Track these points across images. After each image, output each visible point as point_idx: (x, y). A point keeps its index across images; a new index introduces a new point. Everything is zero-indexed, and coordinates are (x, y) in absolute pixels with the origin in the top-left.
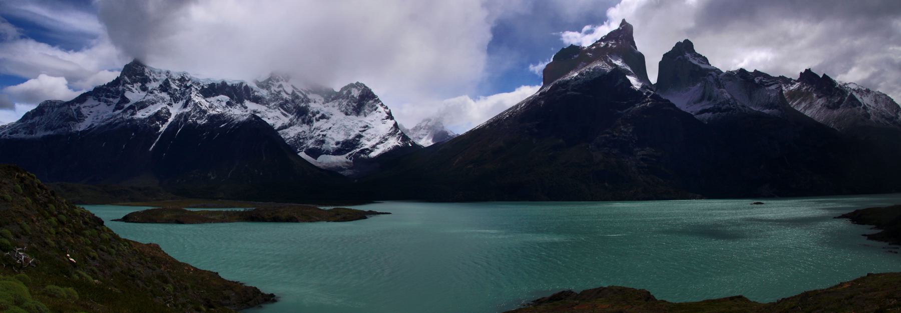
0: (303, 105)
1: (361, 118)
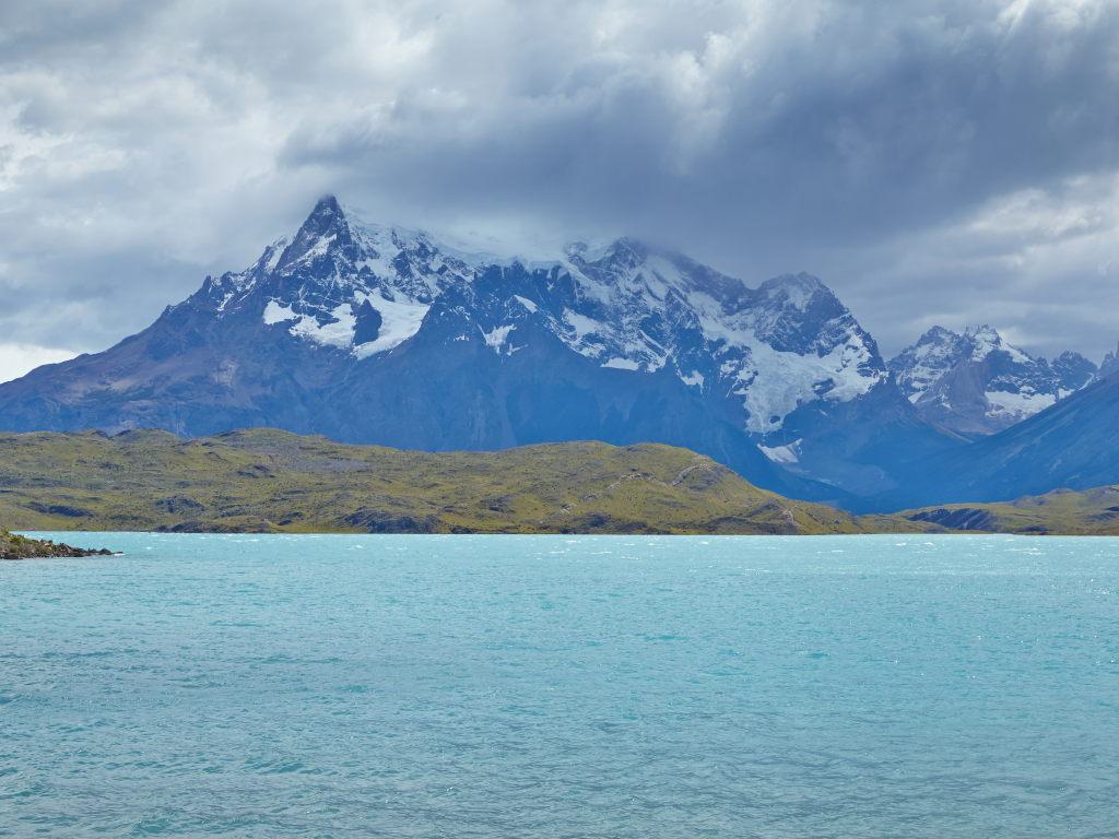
0: (688, 325)
1: (812, 359)
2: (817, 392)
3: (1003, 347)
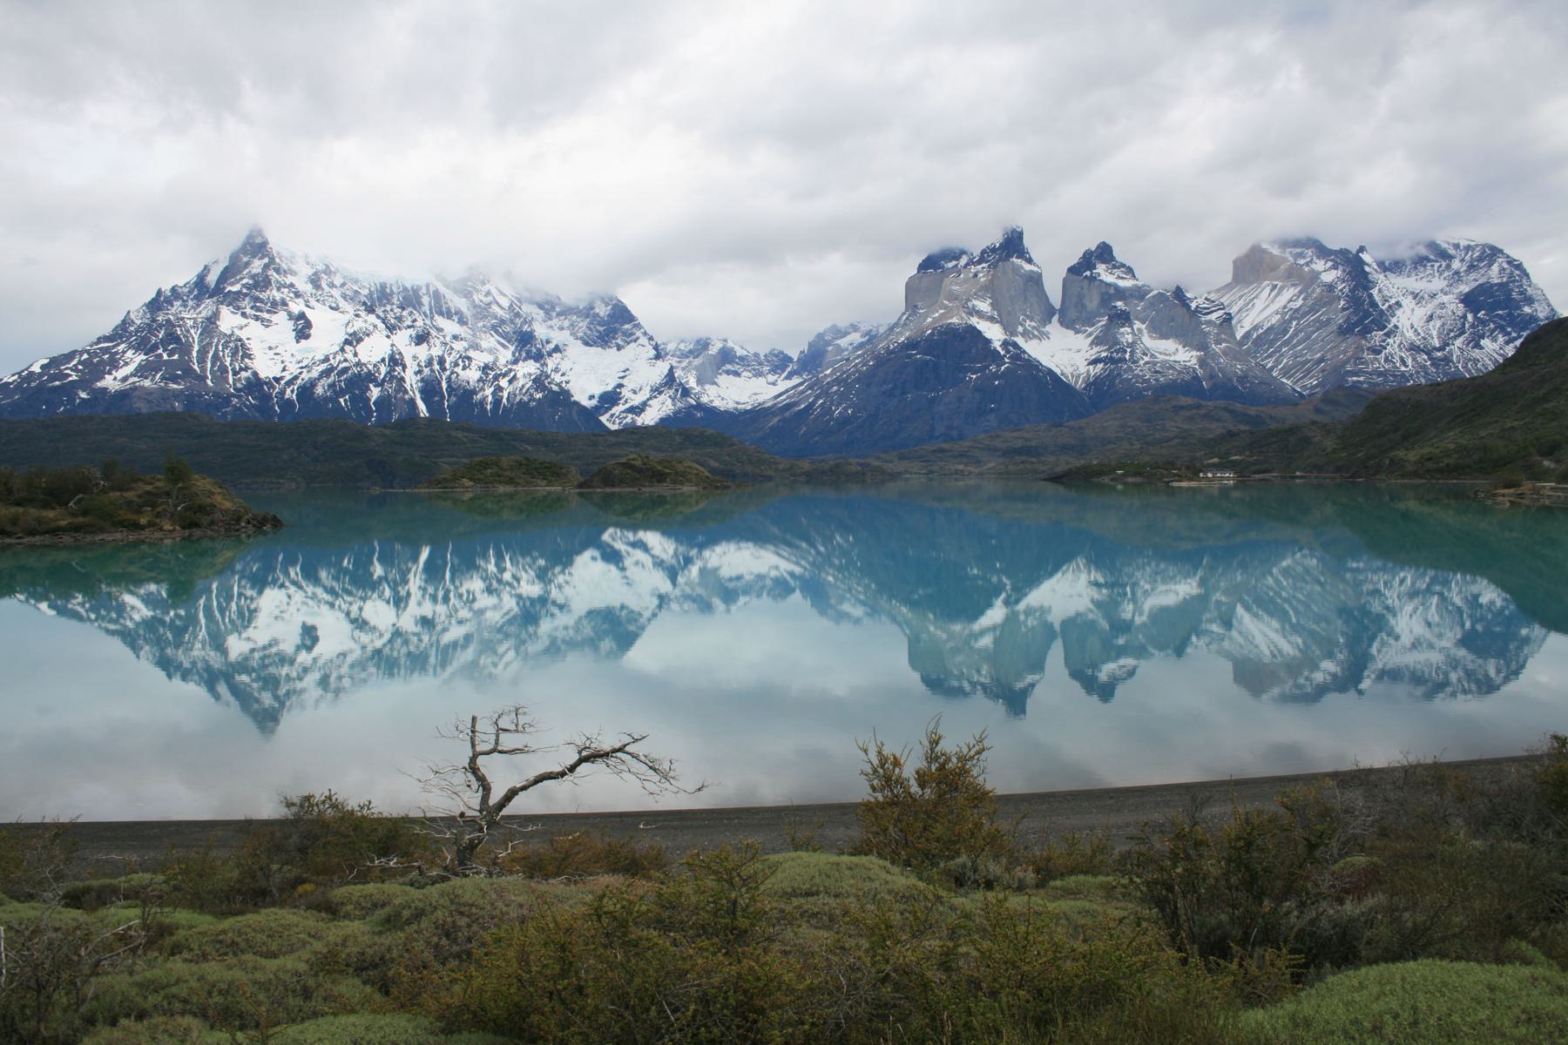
0: (525, 328)
3: (730, 344)
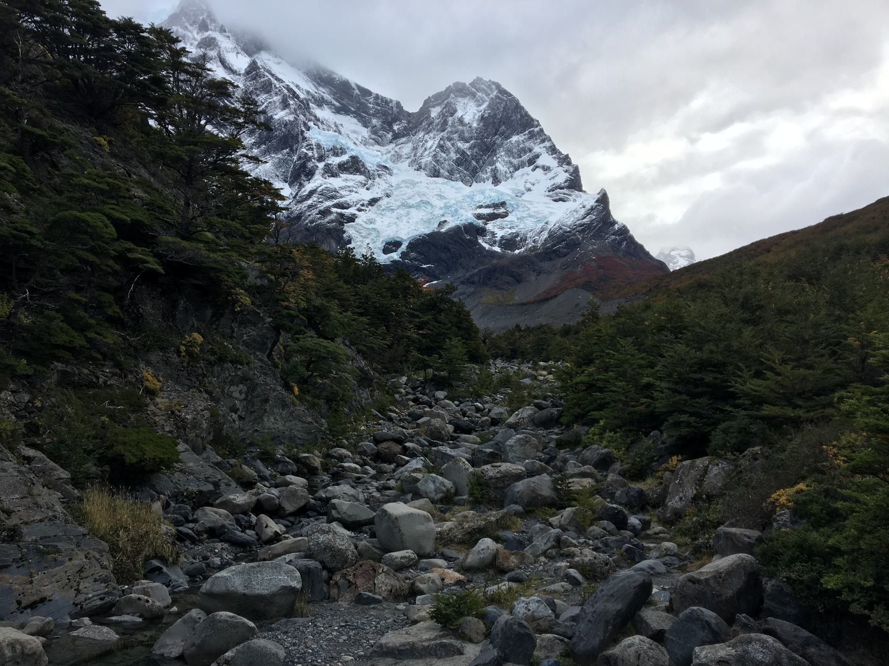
2: (479, 217)
